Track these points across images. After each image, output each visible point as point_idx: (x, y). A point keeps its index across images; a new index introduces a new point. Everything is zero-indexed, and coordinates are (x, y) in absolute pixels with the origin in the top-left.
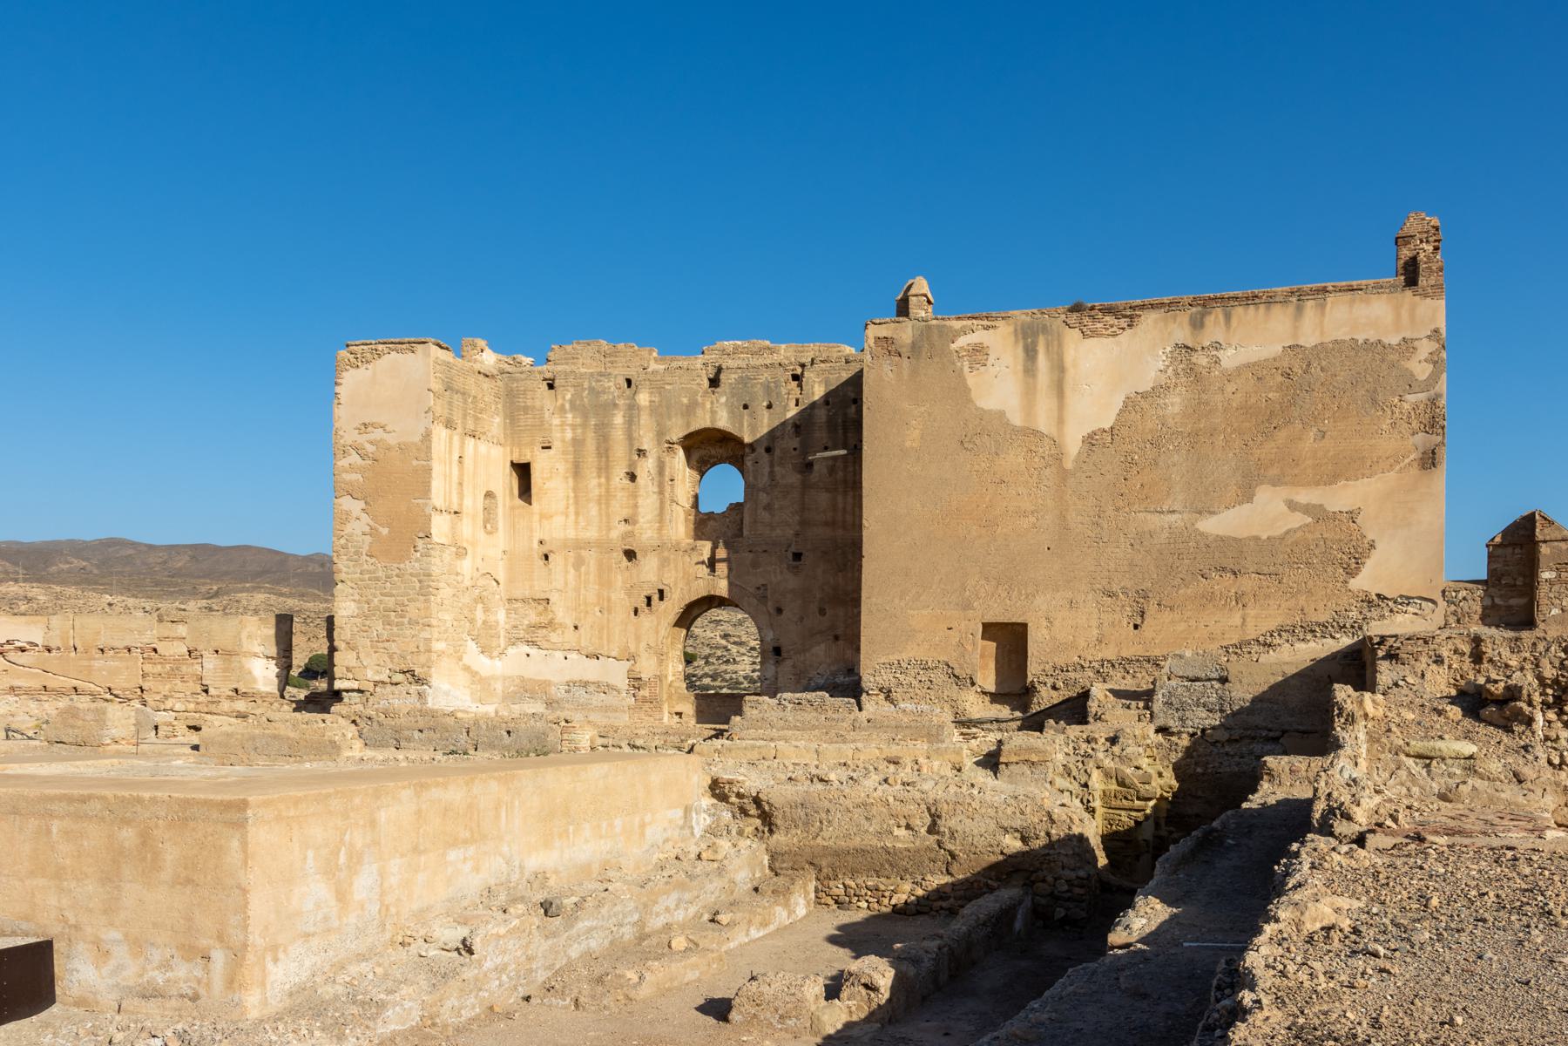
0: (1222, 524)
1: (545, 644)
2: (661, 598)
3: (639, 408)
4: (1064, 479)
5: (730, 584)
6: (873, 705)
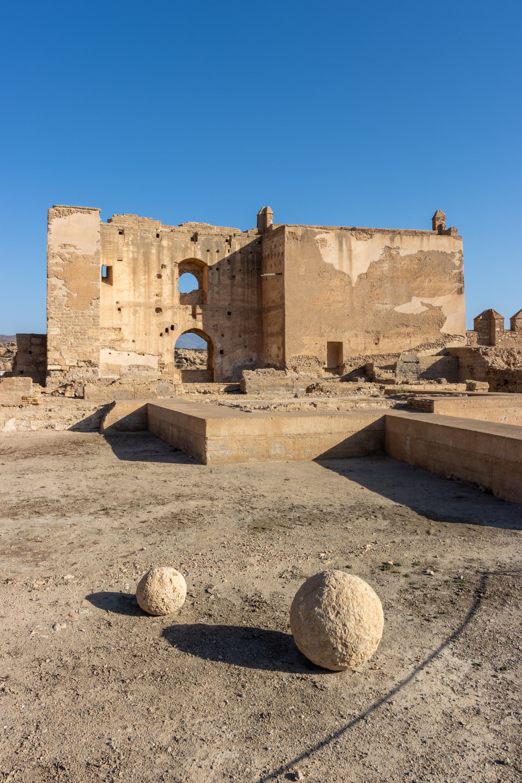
0: (402, 309)
1: (119, 349)
3: (163, 247)
4: (353, 290)
5: (203, 324)
6: (291, 374)
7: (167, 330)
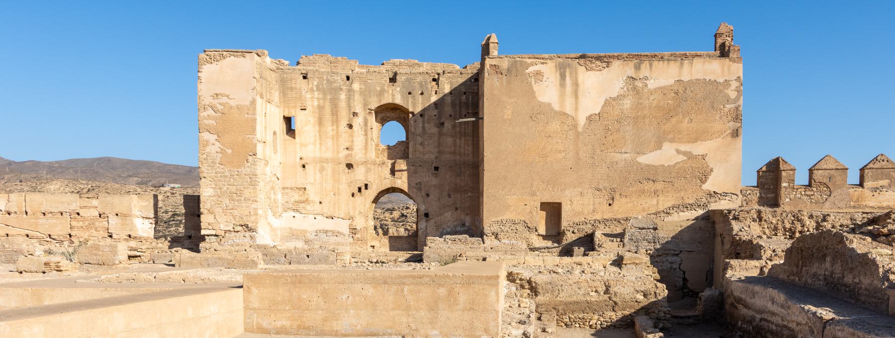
7: (360, 189)
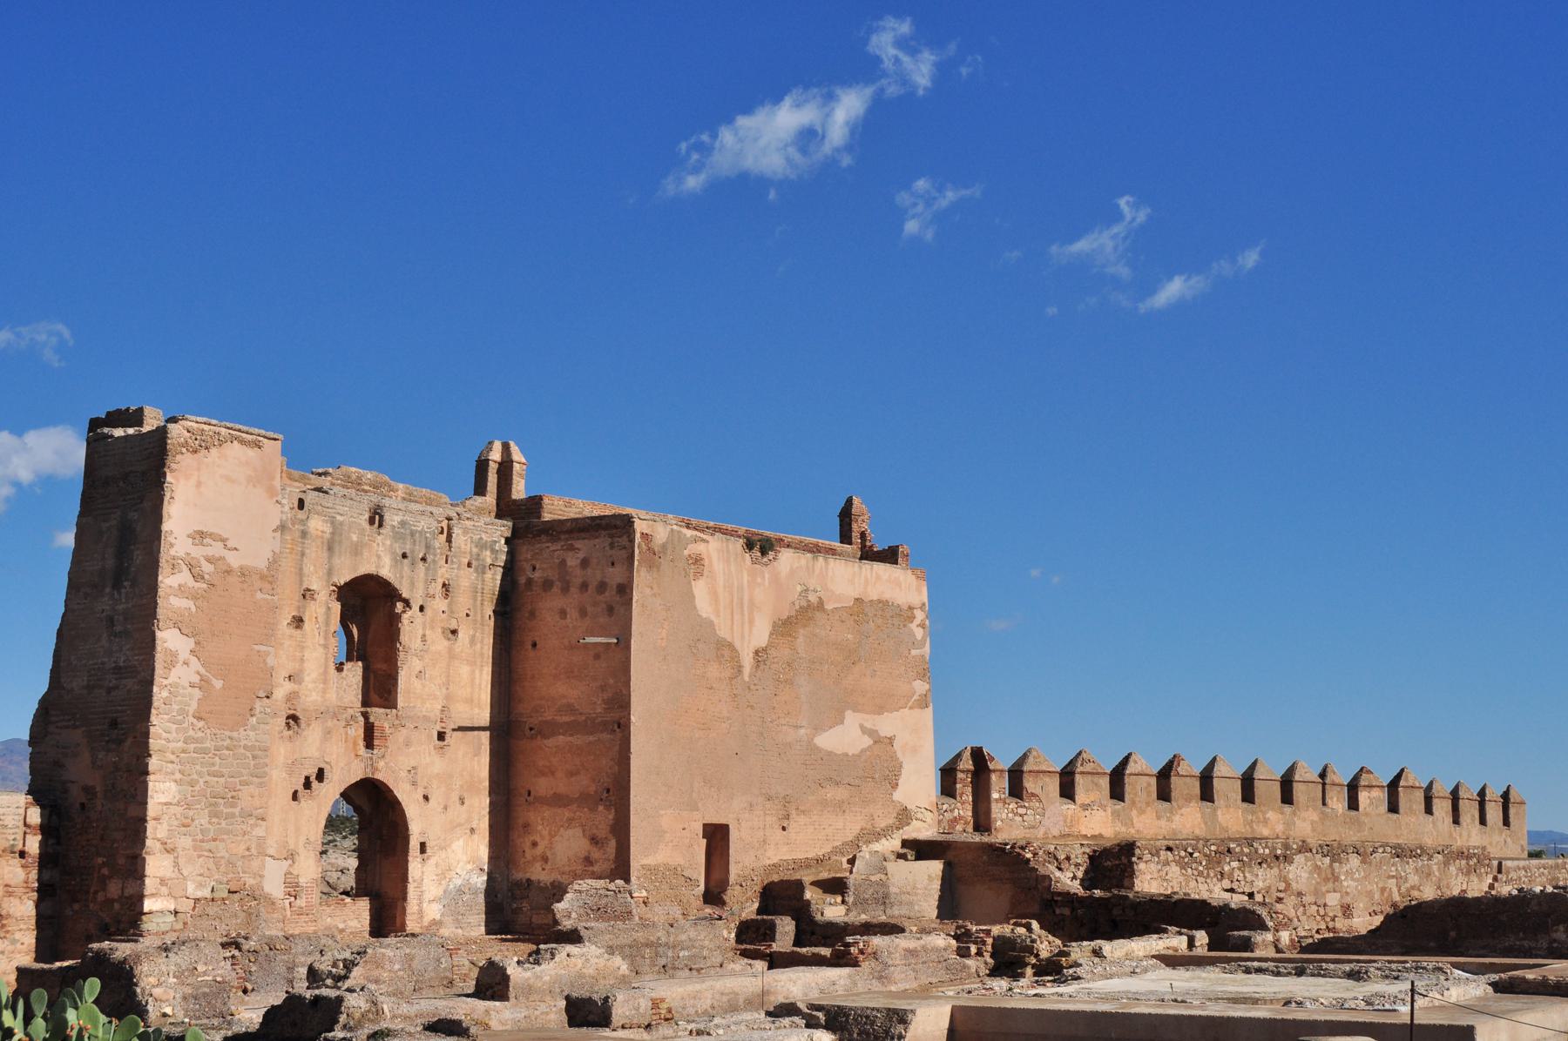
2: (307, 778)
7: (307, 784)
